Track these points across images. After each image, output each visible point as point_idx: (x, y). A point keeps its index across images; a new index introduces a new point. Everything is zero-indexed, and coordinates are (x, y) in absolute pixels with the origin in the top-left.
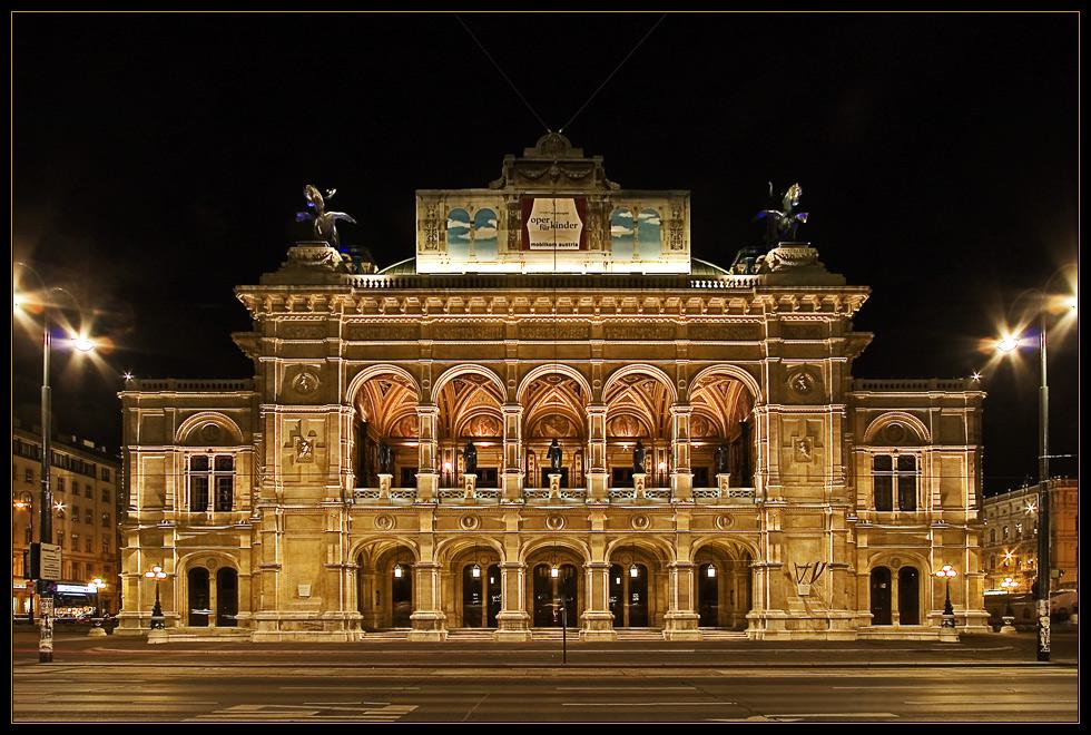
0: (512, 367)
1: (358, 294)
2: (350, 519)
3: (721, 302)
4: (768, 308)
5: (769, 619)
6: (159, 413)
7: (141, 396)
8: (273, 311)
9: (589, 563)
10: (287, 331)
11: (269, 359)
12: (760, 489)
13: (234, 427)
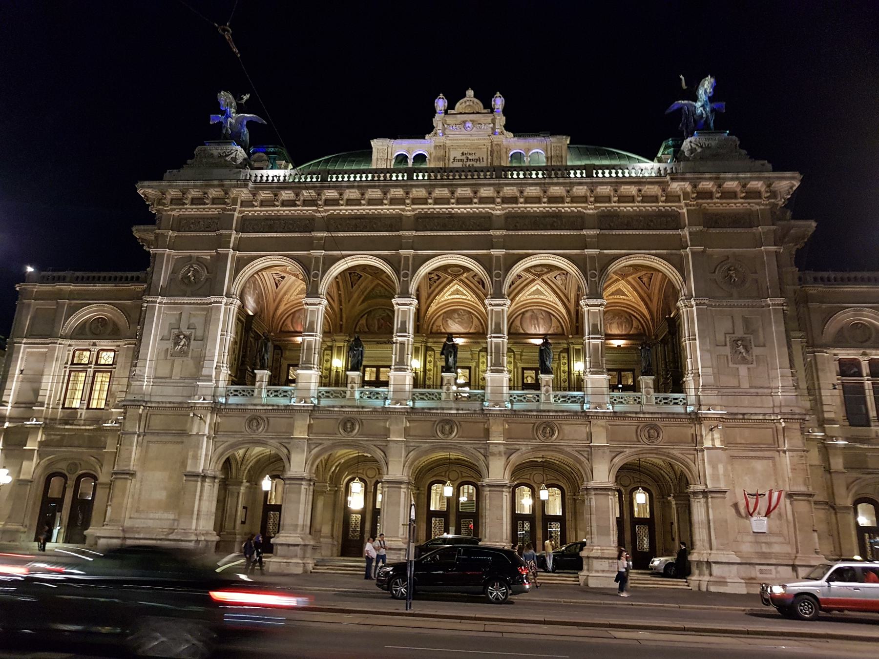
0: (407, 258)
1: (255, 188)
2: (219, 420)
3: (633, 190)
4: (686, 195)
5: (715, 563)
6: (51, 305)
7: (38, 288)
8: (171, 204)
9: (487, 481)
10: (181, 224)
11: (160, 250)
12: (692, 399)
13: (121, 320)
